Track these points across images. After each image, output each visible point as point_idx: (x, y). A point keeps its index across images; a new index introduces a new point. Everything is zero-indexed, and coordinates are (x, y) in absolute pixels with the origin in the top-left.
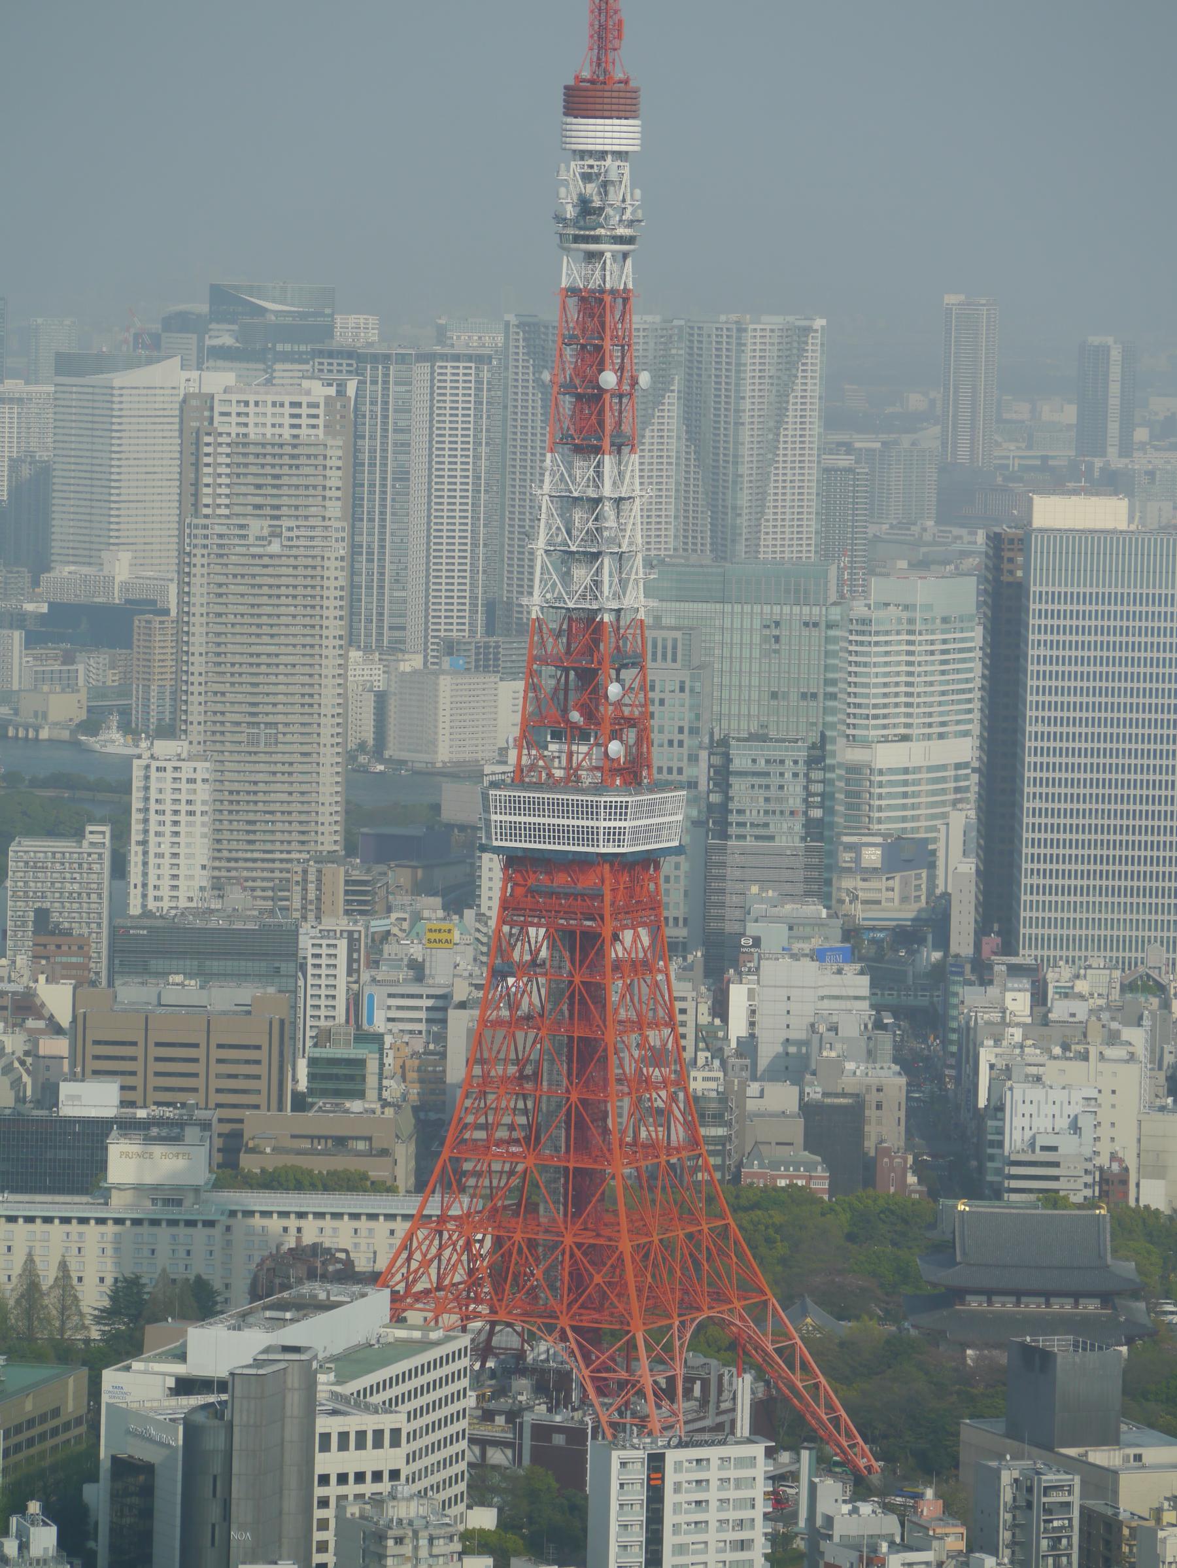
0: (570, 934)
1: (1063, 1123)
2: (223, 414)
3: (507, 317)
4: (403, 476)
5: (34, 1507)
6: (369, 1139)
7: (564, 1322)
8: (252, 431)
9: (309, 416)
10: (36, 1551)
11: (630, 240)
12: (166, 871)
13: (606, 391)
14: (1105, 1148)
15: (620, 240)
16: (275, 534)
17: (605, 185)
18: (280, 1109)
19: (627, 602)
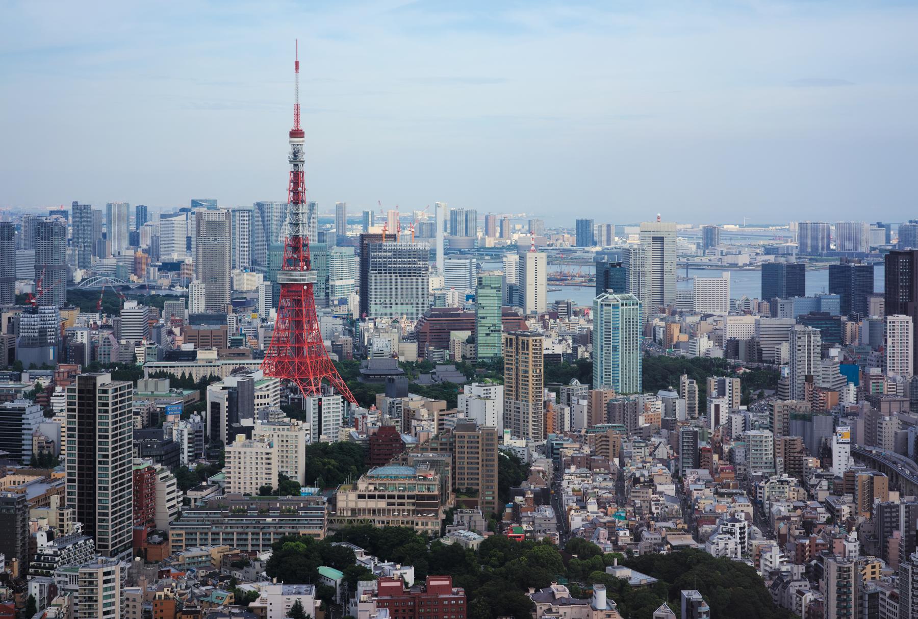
0: (295, 300)
1: (384, 345)
5: (195, 412)
7: (296, 377)
10: (196, 421)
14: (392, 350)
16: (216, 239)
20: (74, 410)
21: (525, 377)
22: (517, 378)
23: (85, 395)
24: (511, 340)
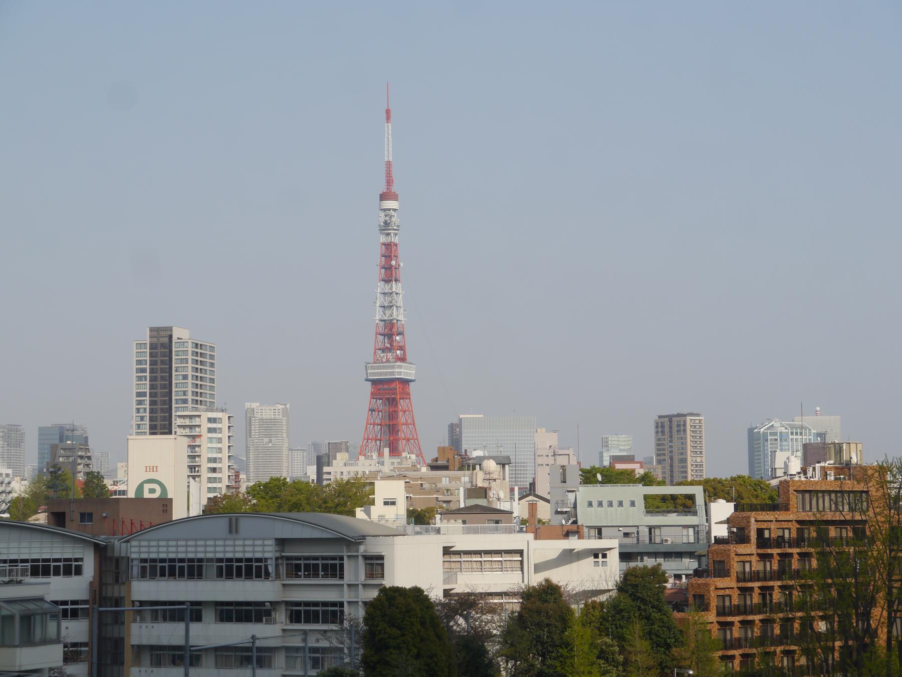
0: (388, 399)
2: (257, 412)
3: (309, 443)
8: (264, 416)
9: (278, 412)
11: (398, 230)
13: (393, 266)
15: (395, 230)
16: (270, 441)
17: (391, 217)
19: (399, 318)
20: (144, 371)
21: (682, 472)
22: (672, 471)
23: (159, 351)
24: (663, 426)
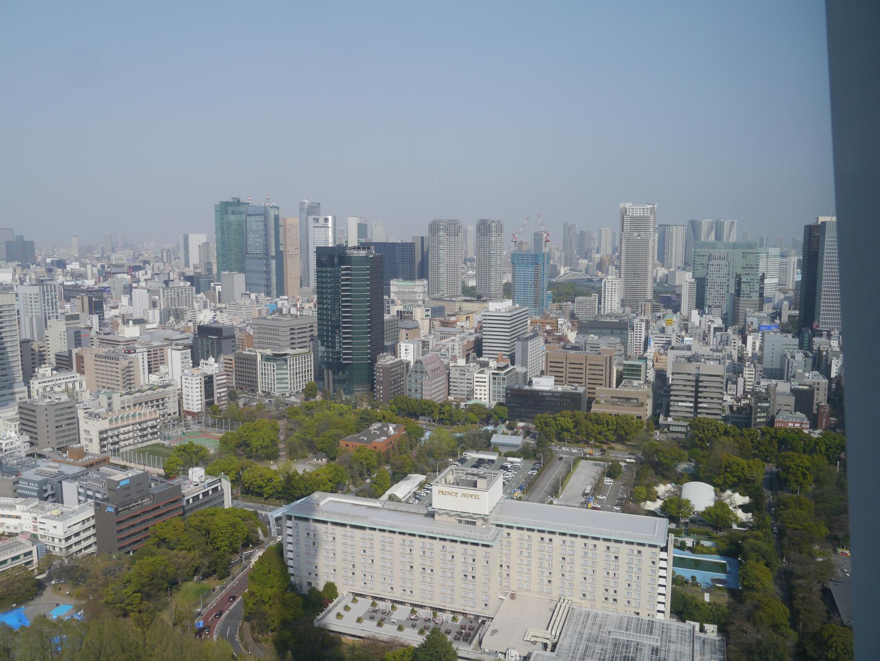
4: (672, 243)
6: (637, 399)
12: (610, 304)
16: (639, 235)
18: (610, 387)
